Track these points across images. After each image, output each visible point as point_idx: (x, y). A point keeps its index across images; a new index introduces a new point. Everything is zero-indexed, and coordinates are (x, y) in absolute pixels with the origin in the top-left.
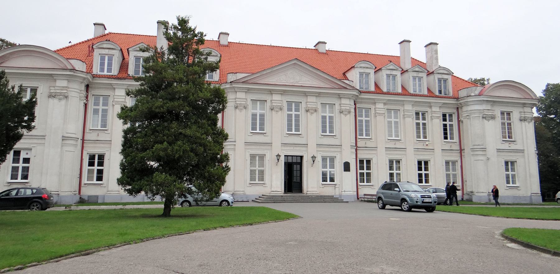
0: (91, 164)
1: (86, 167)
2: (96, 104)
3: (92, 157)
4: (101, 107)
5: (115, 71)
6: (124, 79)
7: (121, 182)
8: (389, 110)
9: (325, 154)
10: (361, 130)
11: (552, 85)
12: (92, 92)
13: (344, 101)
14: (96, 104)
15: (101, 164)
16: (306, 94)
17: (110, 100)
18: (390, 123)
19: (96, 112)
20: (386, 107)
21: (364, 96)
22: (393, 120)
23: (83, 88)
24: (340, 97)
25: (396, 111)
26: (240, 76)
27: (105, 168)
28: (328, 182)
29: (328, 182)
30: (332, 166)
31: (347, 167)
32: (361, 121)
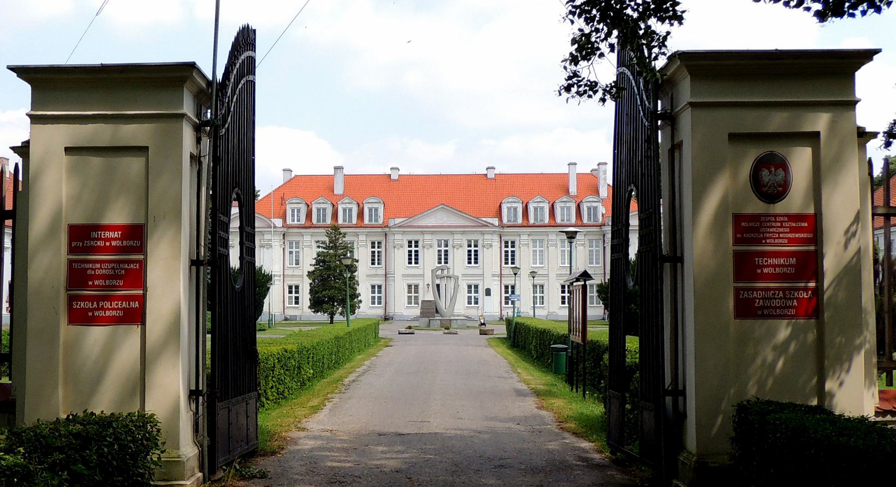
0: (290, 292)
1: (287, 295)
2: (291, 247)
3: (290, 287)
4: (294, 250)
5: (303, 221)
6: (310, 227)
7: (310, 307)
8: (534, 241)
9: (470, 282)
10: (507, 259)
11: (352, 278)
12: (287, 238)
13: (486, 237)
14: (291, 247)
15: (297, 292)
16: (452, 233)
17: (301, 244)
18: (535, 251)
19: (291, 253)
20: (531, 237)
21: (506, 230)
22: (538, 249)
23: (282, 237)
24: (483, 233)
25: (541, 241)
26: (398, 221)
27: (300, 295)
28: (473, 305)
29: (473, 305)
30: (476, 292)
31: (488, 292)
32: (507, 252)
